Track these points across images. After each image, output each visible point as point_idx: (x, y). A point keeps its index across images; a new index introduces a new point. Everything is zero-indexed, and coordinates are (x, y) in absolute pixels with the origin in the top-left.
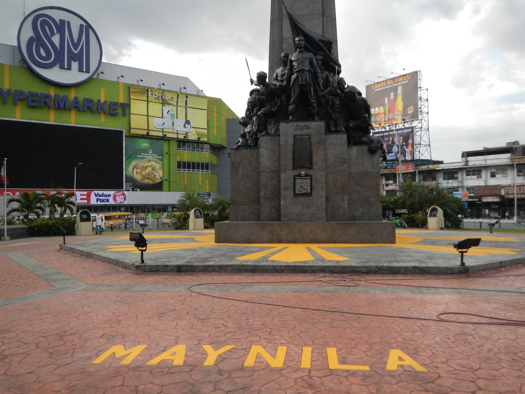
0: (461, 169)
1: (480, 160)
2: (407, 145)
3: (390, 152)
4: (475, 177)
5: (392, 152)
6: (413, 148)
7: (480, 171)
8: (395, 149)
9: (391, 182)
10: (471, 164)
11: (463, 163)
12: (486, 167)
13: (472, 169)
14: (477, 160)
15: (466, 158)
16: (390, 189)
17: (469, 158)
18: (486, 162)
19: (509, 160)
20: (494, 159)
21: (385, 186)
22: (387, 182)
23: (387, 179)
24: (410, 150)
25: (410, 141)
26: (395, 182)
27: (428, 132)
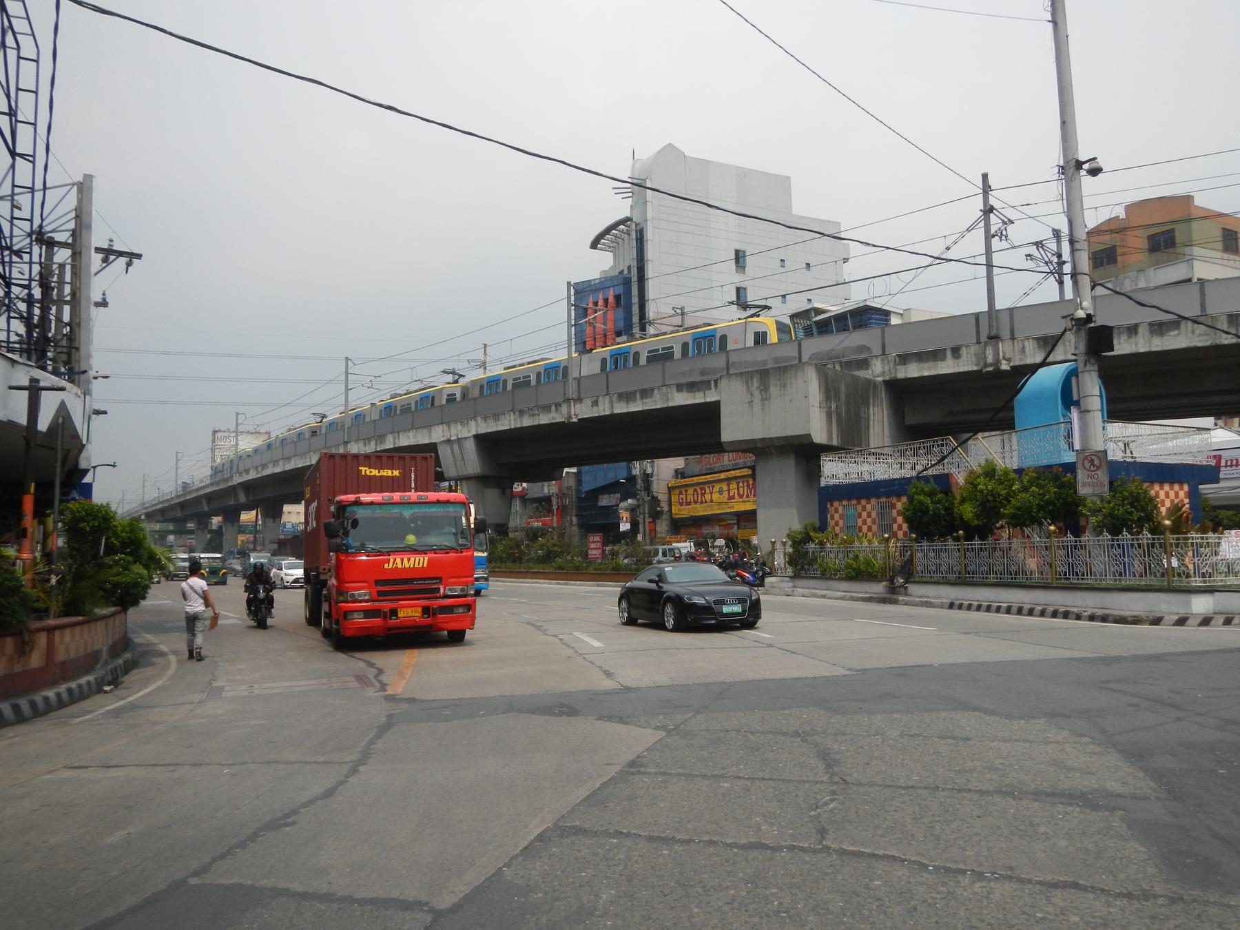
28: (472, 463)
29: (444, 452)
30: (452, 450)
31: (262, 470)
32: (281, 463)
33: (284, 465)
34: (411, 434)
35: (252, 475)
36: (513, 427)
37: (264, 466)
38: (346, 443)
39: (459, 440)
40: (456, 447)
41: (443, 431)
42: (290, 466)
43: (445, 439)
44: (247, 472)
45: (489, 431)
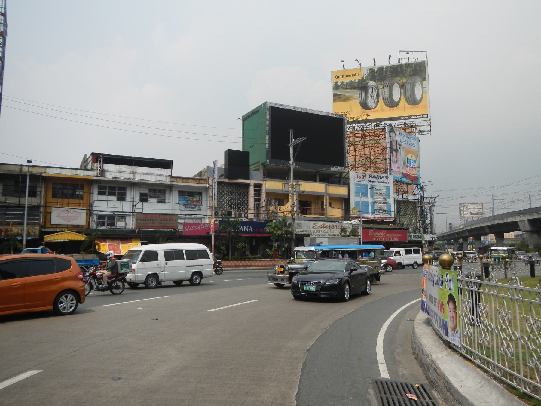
1: (125, 172)
4: (114, 198)
7: (124, 189)
10: (109, 176)
11: (94, 173)
12: (134, 185)
13: (109, 185)
17: (107, 166)
28: (528, 228)
29: (520, 224)
30: (522, 223)
31: (472, 226)
32: (477, 224)
33: (478, 225)
34: (511, 218)
35: (469, 228)
36: (537, 218)
37: (472, 225)
38: (494, 220)
39: (524, 221)
40: (523, 222)
41: (519, 218)
42: (479, 226)
43: (519, 220)
44: (468, 226)
45: (531, 218)
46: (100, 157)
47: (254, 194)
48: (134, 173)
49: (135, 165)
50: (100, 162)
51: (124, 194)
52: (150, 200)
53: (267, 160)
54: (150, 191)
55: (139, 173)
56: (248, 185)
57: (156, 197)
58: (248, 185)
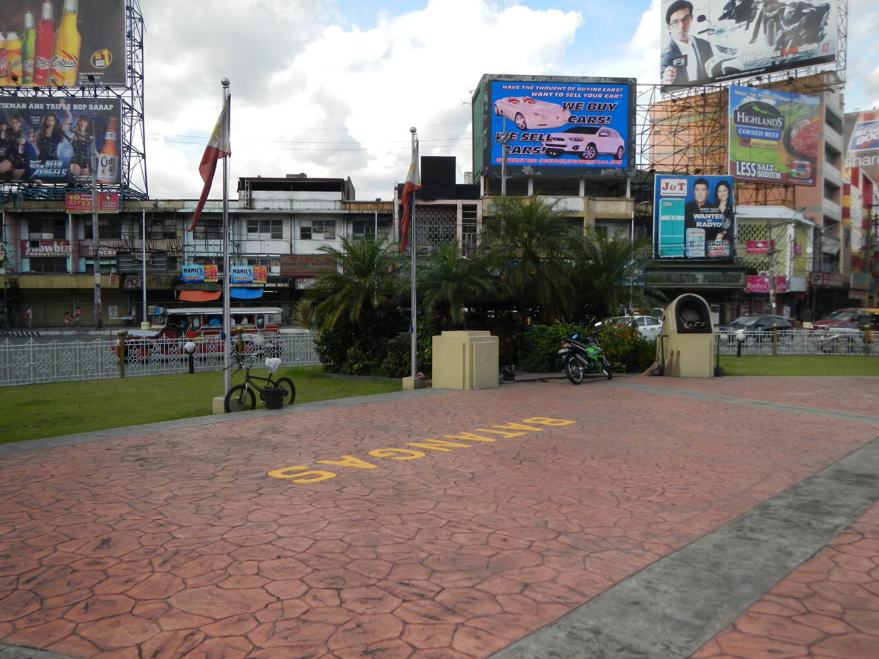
0: (236, 217)
1: (279, 200)
2: (101, 145)
3: (48, 154)
4: (269, 235)
5: (55, 158)
6: (118, 153)
7: (280, 223)
8: (65, 149)
9: (47, 236)
10: (259, 206)
11: (242, 204)
12: (293, 216)
14: (273, 200)
15: (248, 193)
16: (44, 255)
17: (257, 194)
18: (291, 205)
19: (338, 205)
20: (309, 200)
21: (28, 245)
22: (35, 236)
23: (33, 229)
24: (109, 158)
25: (110, 136)
26: (60, 236)
27: (141, 122)
46: (247, 183)
47: (463, 221)
48: (291, 201)
49: (294, 190)
50: (247, 190)
51: (281, 230)
52: (315, 236)
53: (484, 166)
54: (314, 223)
55: (298, 201)
56: (454, 207)
57: (322, 232)
58: (454, 207)
